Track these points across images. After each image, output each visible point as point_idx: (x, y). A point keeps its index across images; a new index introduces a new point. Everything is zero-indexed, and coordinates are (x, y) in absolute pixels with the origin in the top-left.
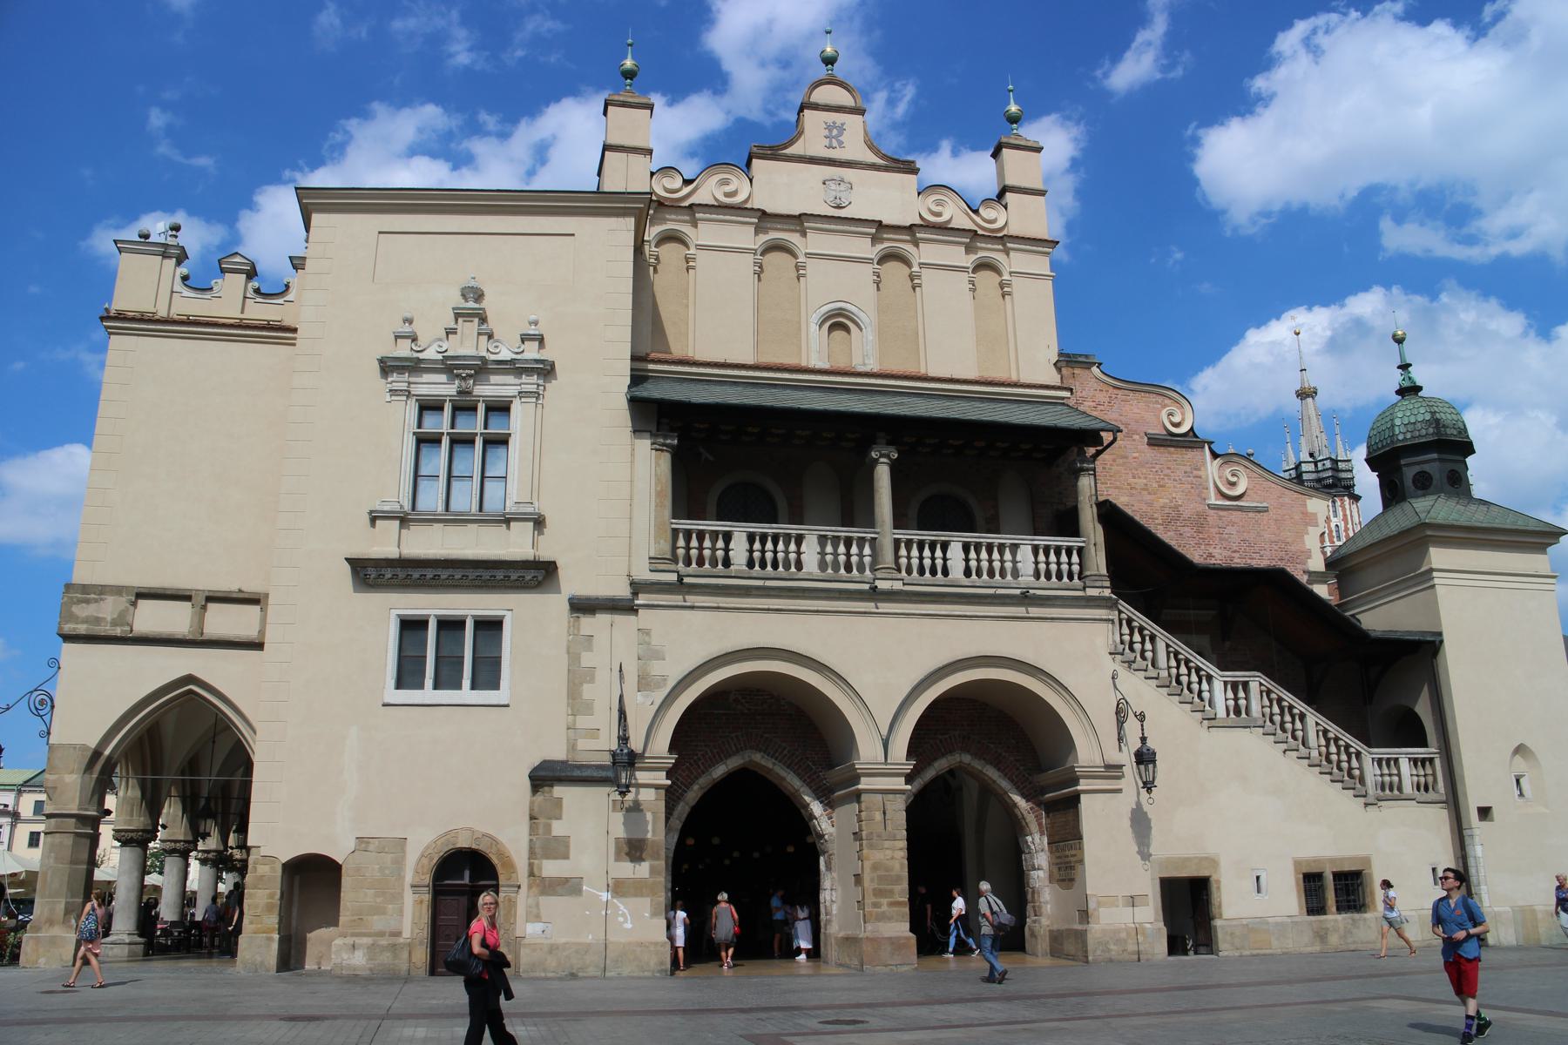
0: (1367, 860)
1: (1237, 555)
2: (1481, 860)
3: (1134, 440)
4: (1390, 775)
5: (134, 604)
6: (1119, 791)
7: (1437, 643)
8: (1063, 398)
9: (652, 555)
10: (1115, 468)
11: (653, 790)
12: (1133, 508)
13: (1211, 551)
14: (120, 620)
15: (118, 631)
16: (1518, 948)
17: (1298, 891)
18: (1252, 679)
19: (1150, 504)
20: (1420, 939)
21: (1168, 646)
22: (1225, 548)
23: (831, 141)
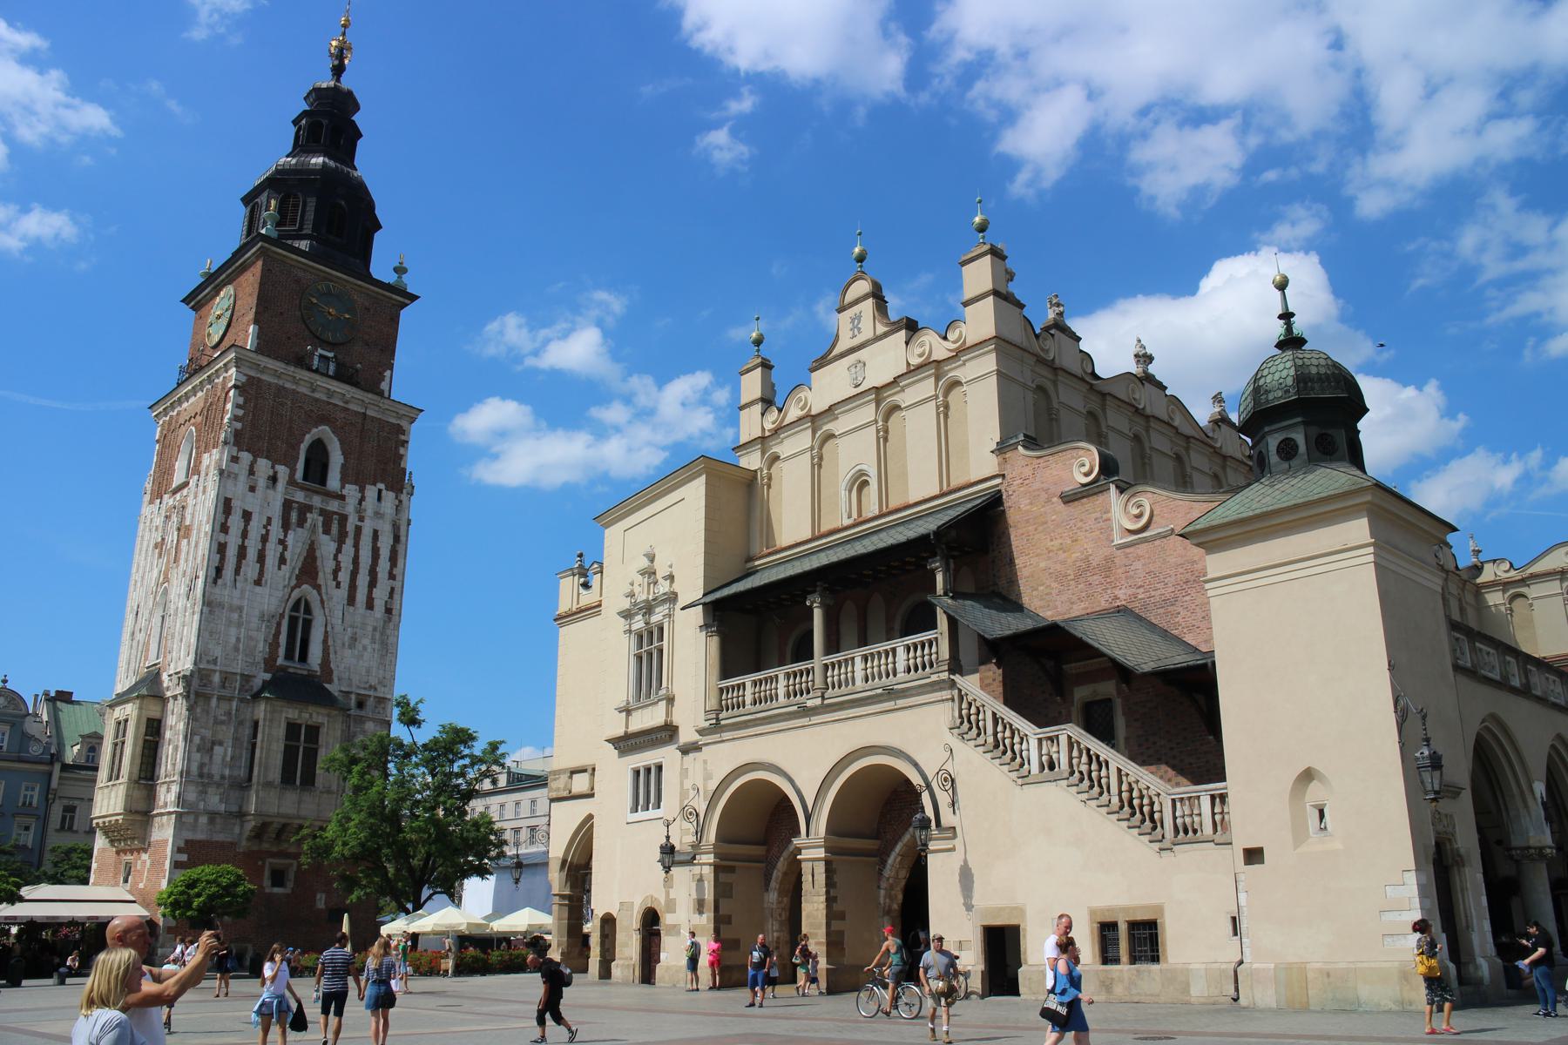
1: (1142, 590)
2: (1245, 909)
3: (1053, 503)
4: (1191, 815)
5: (571, 777)
6: (953, 849)
7: (1210, 665)
8: (997, 485)
9: (707, 709)
10: (1037, 537)
12: (1051, 571)
13: (1116, 593)
15: (565, 794)
16: (1278, 1011)
17: (1093, 939)
18: (1060, 732)
19: (1063, 562)
20: (1206, 995)
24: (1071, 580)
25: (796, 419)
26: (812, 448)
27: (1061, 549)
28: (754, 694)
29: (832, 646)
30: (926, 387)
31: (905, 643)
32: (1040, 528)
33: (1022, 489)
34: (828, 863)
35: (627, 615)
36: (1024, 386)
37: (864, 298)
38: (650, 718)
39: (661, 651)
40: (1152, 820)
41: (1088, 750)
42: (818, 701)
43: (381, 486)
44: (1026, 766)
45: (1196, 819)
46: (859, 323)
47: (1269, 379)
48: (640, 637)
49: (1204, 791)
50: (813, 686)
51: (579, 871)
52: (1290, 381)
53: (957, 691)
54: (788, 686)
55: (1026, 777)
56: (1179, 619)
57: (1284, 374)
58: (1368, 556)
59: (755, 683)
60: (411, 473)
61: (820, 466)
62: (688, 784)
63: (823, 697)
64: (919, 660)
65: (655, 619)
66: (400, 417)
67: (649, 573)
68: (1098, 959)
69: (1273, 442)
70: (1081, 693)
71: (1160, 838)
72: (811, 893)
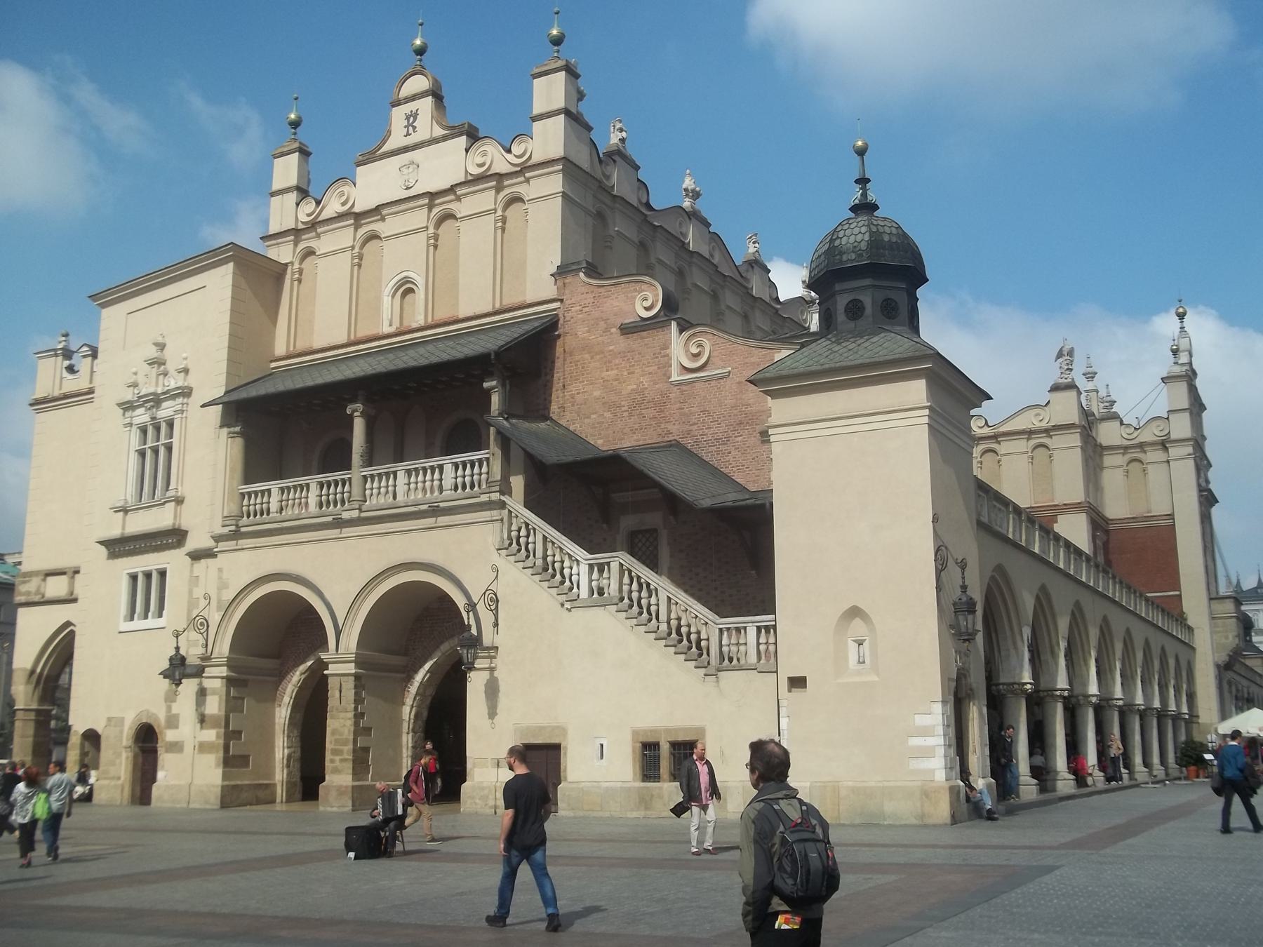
0: (701, 731)
2: (786, 732)
3: (612, 334)
4: (738, 644)
7: (768, 504)
8: (555, 310)
9: (225, 514)
11: (220, 680)
13: (669, 428)
14: (38, 592)
15: (37, 598)
17: (634, 759)
18: (612, 559)
21: (545, 538)
22: (684, 422)
23: (408, 131)
24: (625, 411)
25: (336, 215)
27: (616, 380)
28: (282, 501)
29: (369, 460)
30: (485, 199)
31: (454, 461)
32: (598, 357)
33: (580, 316)
34: (357, 677)
37: (423, 95)
38: (159, 519)
40: (699, 647)
41: (639, 578)
44: (575, 590)
45: (742, 648)
46: (414, 121)
47: (844, 240)
48: (144, 431)
49: (751, 624)
50: (350, 497)
52: (863, 246)
53: (506, 511)
54: (321, 496)
55: (576, 600)
56: (730, 458)
57: (859, 237)
58: (923, 417)
59: (282, 490)
61: (360, 266)
62: (198, 592)
64: (468, 479)
67: (157, 362)
68: (639, 776)
69: (842, 302)
70: (628, 522)
71: (706, 663)
72: (337, 709)
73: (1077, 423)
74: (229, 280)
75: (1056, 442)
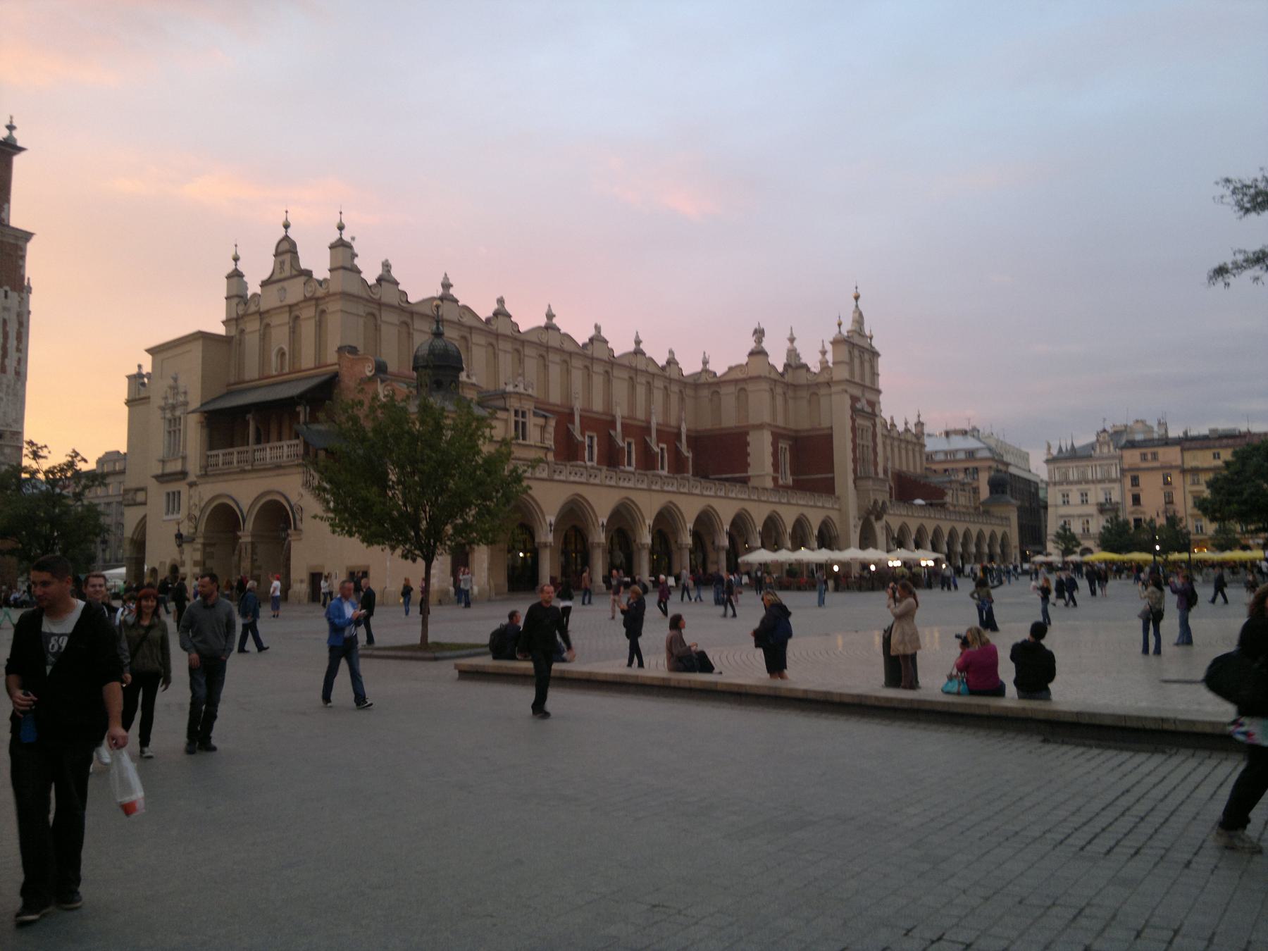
0: (368, 567)
5: (135, 493)
26: (260, 330)
29: (258, 441)
35: (163, 409)
36: (358, 315)
38: (176, 466)
39: (180, 430)
42: (250, 467)
43: (7, 288)
48: (170, 421)
51: (139, 544)
60: (29, 279)
62: (192, 502)
63: (252, 465)
65: (178, 413)
66: (17, 238)
73: (763, 375)
74: (200, 348)
75: (750, 387)
